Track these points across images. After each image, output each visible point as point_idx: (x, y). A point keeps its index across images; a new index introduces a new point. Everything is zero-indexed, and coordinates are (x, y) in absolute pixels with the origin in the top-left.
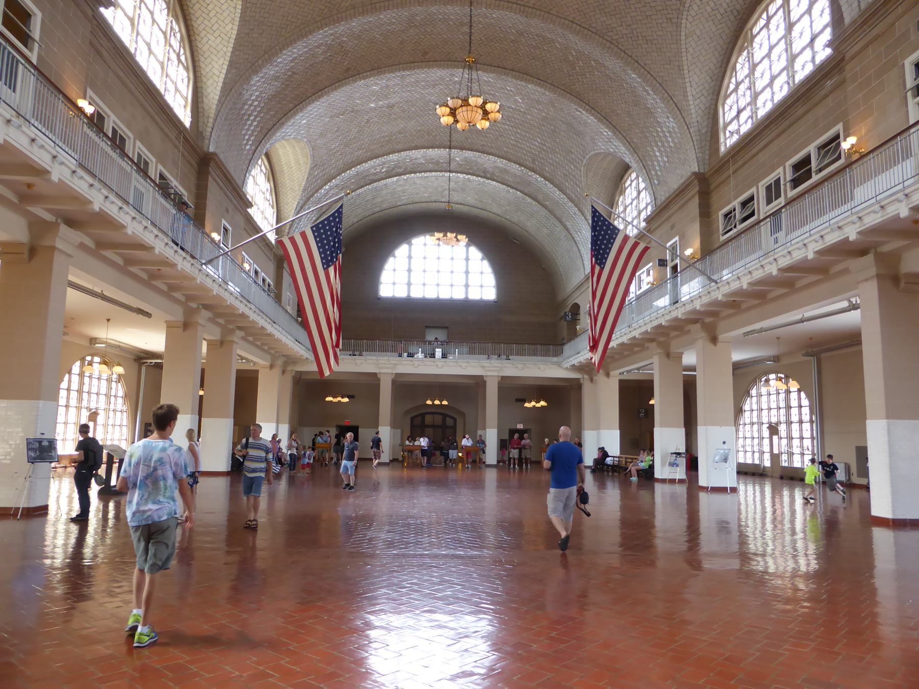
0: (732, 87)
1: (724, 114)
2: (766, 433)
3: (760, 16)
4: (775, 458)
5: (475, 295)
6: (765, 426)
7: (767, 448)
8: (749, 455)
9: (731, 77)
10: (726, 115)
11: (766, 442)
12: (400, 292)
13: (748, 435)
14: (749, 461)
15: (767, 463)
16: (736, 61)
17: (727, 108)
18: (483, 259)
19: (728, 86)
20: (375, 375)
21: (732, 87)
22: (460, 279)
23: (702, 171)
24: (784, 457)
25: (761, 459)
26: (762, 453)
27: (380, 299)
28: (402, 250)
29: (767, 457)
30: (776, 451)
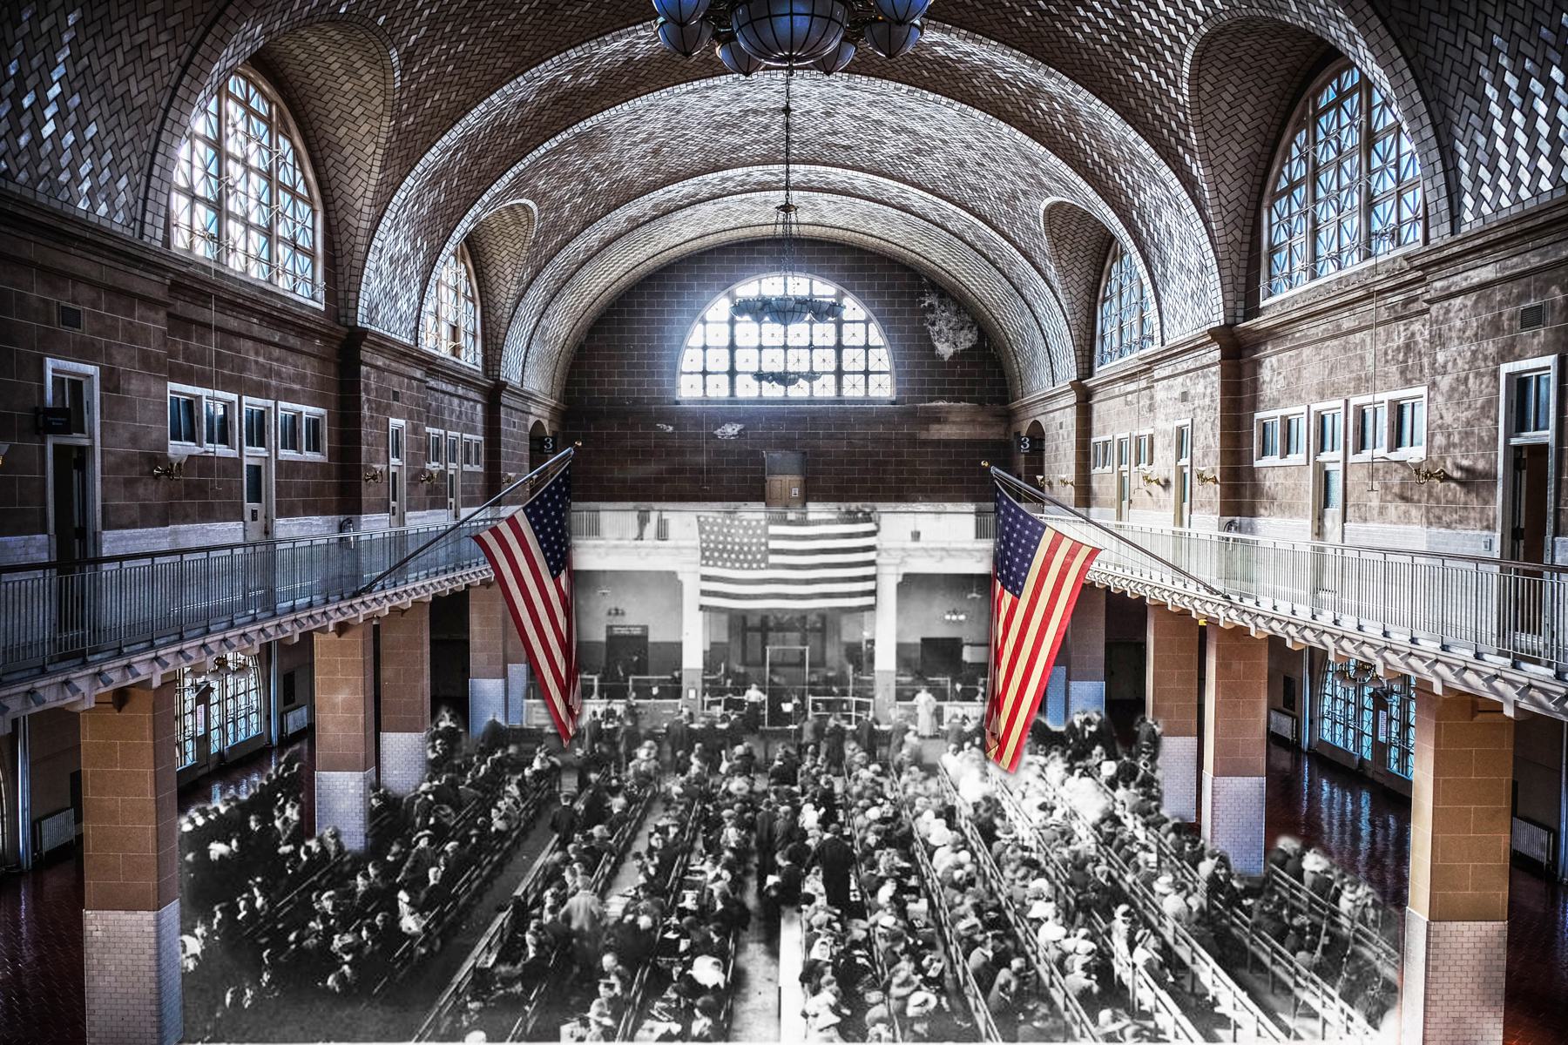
0: (1284, 184)
1: (1270, 226)
2: (1368, 702)
3: (1328, 82)
4: (1380, 749)
5: (853, 389)
6: (1368, 690)
7: (1368, 729)
8: (1339, 729)
9: (1283, 164)
10: (1275, 228)
11: (1368, 716)
12: (718, 389)
13: (1339, 692)
14: (1340, 744)
15: (1368, 756)
16: (1292, 140)
17: (1275, 219)
18: (867, 322)
19: (1278, 180)
20: (674, 573)
21: (1284, 184)
22: (825, 360)
23: (1230, 320)
24: (1394, 753)
25: (1358, 746)
26: (1360, 735)
27: (677, 403)
28: (720, 308)
29: (1367, 741)
30: (1382, 738)
